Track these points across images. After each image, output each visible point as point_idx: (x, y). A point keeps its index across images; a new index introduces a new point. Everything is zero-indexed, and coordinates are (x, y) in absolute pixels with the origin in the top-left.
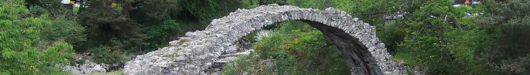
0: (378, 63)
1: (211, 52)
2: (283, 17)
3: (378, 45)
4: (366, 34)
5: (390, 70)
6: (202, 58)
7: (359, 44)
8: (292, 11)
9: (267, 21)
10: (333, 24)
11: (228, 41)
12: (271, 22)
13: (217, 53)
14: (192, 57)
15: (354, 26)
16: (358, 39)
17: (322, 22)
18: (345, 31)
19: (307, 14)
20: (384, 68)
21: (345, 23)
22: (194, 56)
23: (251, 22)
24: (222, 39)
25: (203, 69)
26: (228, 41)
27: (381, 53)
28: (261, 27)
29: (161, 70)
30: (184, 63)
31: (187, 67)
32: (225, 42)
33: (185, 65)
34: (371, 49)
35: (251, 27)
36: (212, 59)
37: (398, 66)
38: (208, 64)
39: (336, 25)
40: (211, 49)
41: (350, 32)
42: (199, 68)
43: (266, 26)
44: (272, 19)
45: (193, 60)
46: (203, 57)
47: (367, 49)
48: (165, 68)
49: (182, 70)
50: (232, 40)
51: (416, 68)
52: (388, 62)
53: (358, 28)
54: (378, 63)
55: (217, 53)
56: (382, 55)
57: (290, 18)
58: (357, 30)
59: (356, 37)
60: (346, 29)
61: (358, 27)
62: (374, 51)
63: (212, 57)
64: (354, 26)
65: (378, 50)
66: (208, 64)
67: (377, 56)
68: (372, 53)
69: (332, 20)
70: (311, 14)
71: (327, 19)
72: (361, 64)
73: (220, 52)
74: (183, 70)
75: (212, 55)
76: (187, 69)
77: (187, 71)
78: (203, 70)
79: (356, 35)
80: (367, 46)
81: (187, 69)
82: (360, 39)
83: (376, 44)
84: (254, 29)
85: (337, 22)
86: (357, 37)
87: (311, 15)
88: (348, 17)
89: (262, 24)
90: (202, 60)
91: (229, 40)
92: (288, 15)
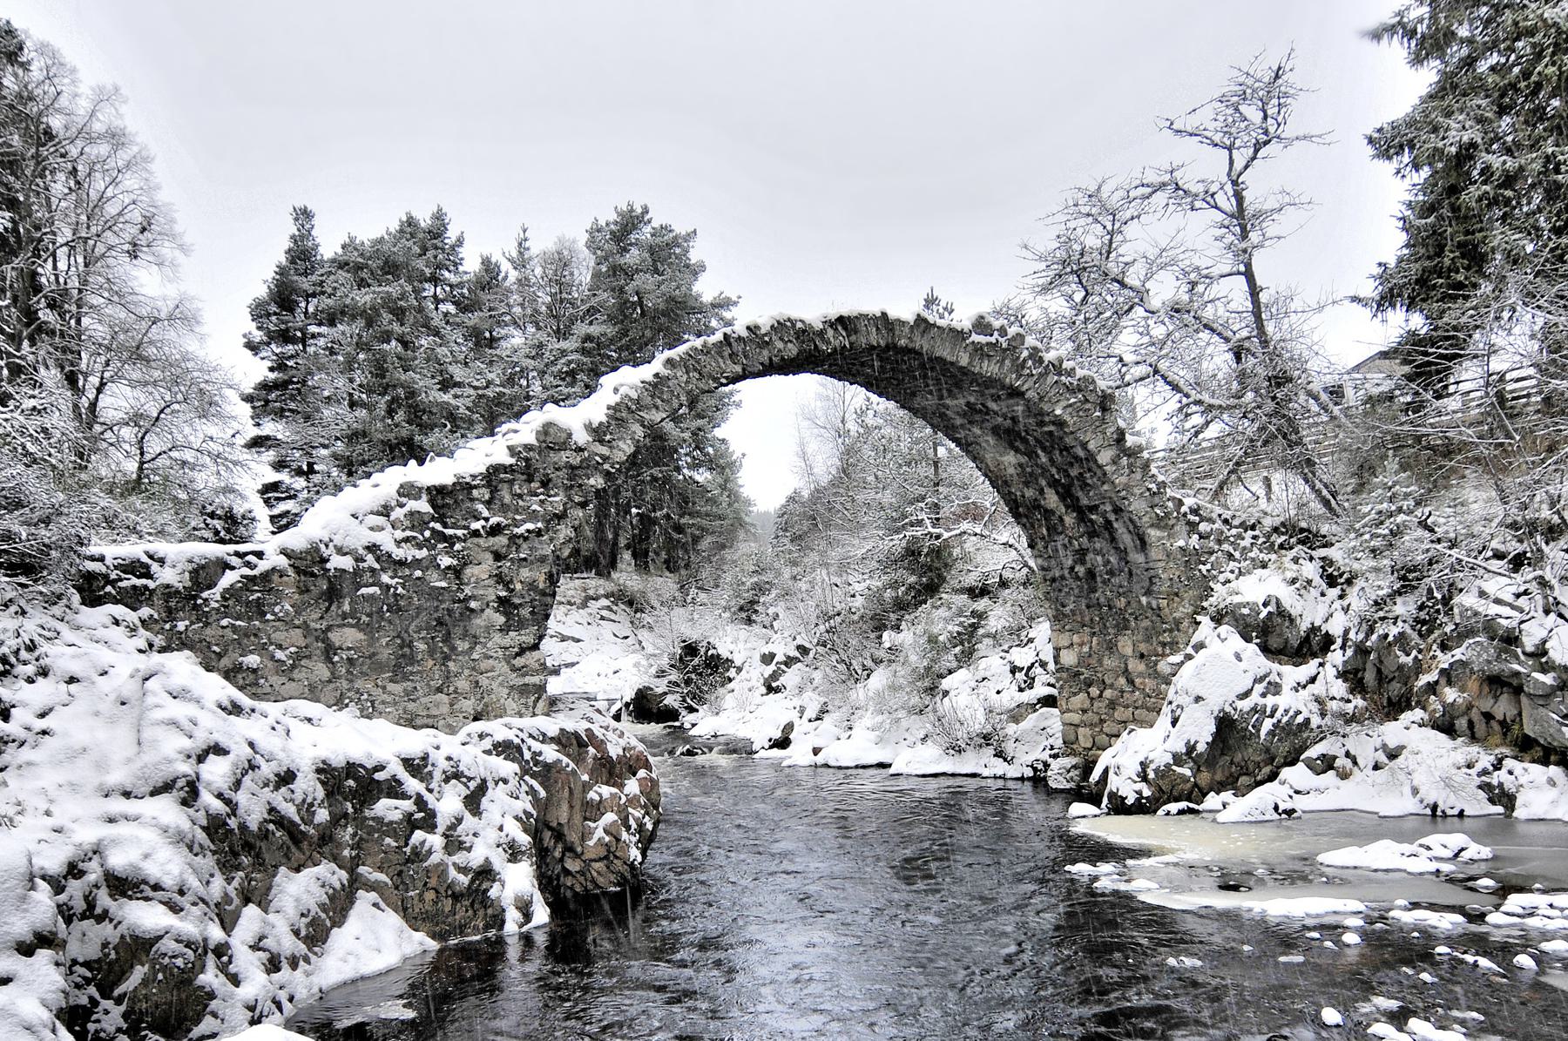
6: (571, 460)
9: (780, 345)
12: (792, 350)
13: (621, 444)
20: (1145, 519)
25: (577, 499)
26: (657, 408)
28: (762, 364)
31: (518, 491)
32: (648, 408)
35: (729, 362)
38: (592, 481)
63: (605, 459)
66: (592, 481)
68: (1107, 468)
72: (1069, 520)
73: (629, 442)
74: (507, 499)
75: (604, 450)
77: (521, 503)
81: (520, 496)
90: (573, 468)
91: (659, 402)
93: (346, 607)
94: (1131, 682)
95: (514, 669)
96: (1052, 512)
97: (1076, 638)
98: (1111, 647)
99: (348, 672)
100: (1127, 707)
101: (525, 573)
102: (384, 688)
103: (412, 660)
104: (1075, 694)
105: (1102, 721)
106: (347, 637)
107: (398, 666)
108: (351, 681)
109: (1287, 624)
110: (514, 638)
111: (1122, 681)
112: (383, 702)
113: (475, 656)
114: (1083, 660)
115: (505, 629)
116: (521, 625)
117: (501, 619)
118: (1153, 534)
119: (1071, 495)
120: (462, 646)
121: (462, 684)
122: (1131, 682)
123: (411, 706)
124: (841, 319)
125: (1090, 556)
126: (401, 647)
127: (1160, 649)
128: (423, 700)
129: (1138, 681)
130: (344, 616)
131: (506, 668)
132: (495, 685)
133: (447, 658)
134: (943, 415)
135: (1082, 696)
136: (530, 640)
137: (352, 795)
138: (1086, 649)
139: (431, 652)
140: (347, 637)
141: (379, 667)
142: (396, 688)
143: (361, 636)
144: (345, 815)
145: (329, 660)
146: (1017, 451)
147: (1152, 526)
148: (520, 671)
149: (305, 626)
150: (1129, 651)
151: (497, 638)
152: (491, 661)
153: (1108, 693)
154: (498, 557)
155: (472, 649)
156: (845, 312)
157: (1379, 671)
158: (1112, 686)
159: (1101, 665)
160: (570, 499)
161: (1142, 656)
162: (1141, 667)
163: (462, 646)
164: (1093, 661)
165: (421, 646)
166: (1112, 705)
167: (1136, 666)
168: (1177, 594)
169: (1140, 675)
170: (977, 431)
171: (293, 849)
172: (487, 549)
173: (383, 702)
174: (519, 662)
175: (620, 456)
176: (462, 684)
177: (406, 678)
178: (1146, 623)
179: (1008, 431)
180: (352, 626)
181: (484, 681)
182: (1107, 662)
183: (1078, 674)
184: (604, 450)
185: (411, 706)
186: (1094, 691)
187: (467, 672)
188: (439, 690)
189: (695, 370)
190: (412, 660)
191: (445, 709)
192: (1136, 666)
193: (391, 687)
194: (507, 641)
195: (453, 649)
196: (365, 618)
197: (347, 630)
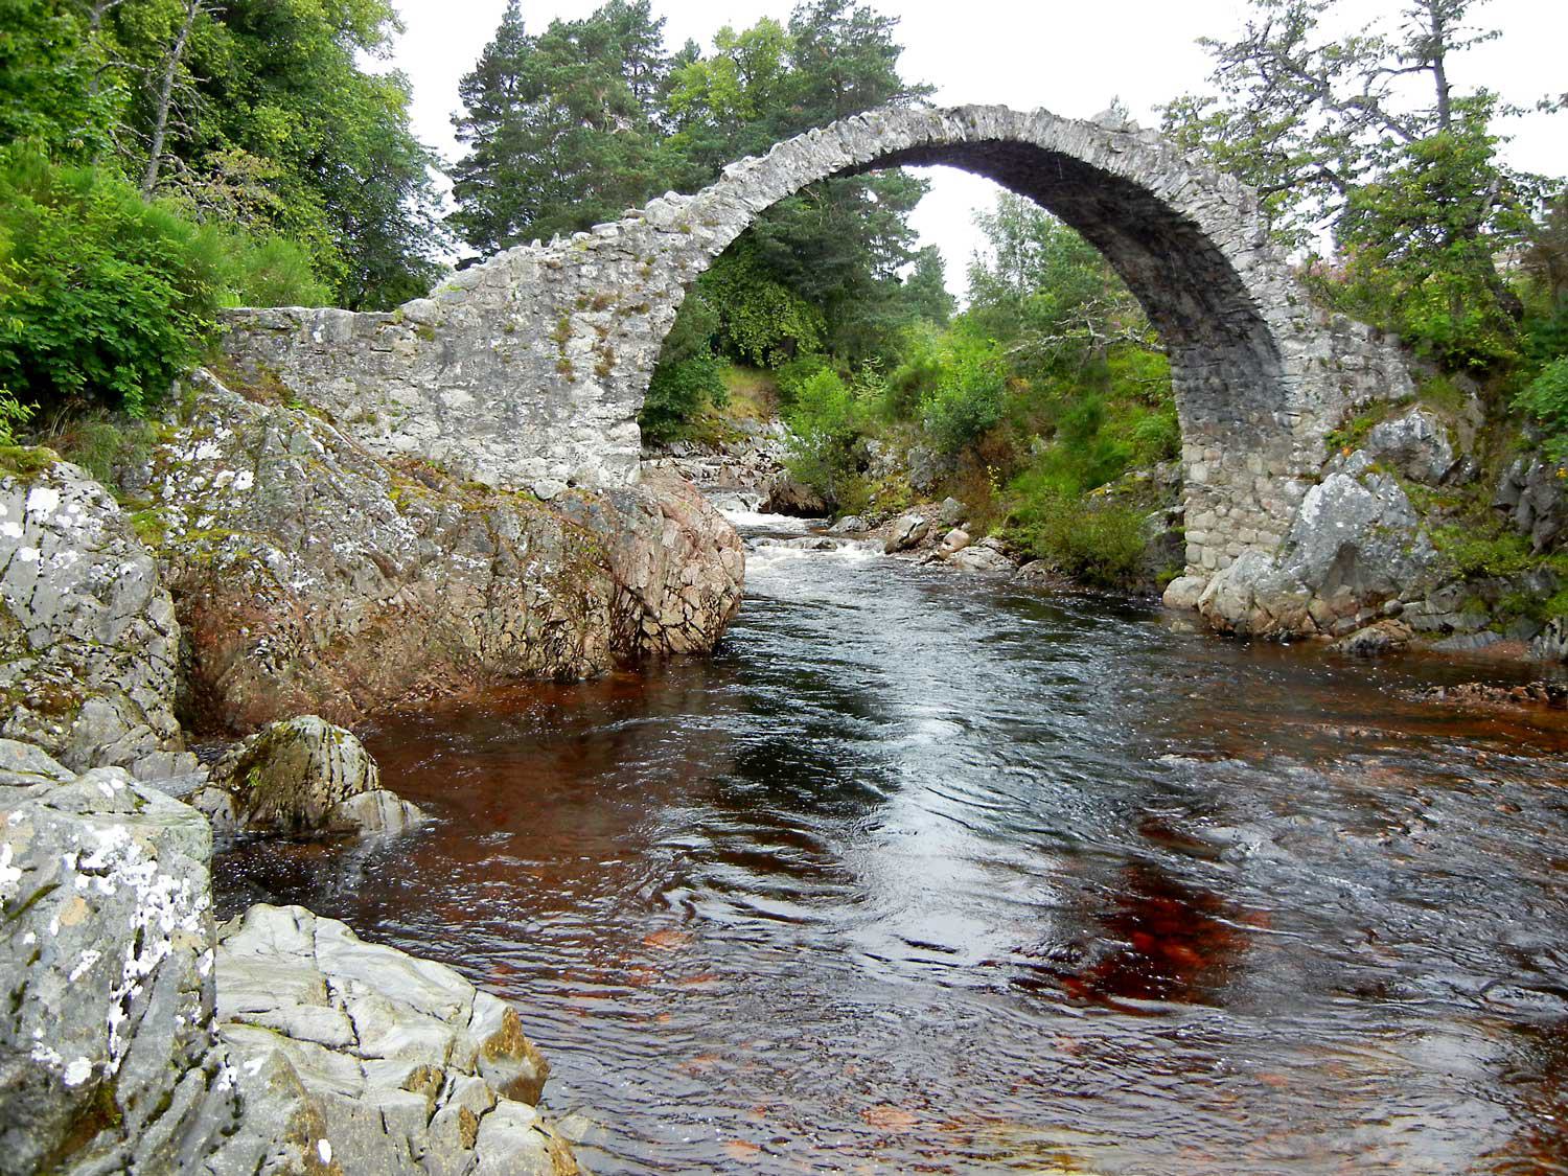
0: (1261, 311)
1: (706, 225)
2: (946, 123)
3: (1265, 250)
4: (1223, 208)
5: (1302, 336)
7: (1202, 243)
9: (892, 136)
10: (1116, 165)
11: (763, 194)
14: (641, 236)
15: (1184, 178)
16: (1195, 225)
17: (1076, 155)
18: (1152, 192)
19: (1028, 123)
20: (1282, 330)
21: (1154, 165)
22: (648, 233)
23: (841, 134)
25: (680, 280)
26: (763, 194)
27: (1271, 280)
30: (614, 256)
34: (1239, 263)
36: (711, 250)
37: (1327, 327)
38: (696, 264)
39: (1123, 167)
41: (1172, 199)
42: (666, 276)
43: (888, 151)
44: (911, 130)
45: (645, 246)
46: (681, 241)
47: (1224, 262)
49: (608, 276)
50: (776, 188)
51: (1388, 339)
52: (1297, 310)
53: (1196, 187)
54: (1261, 311)
55: (727, 229)
56: (1278, 283)
57: (971, 130)
59: (1191, 216)
60: (1160, 188)
61: (1198, 183)
62: (1251, 269)
63: (706, 243)
64: (1184, 178)
65: (1262, 268)
66: (696, 264)
67: (1260, 287)
69: (1112, 151)
70: (1043, 123)
71: (1096, 143)
74: (614, 277)
75: (708, 234)
78: (682, 285)
79: (1190, 210)
80: (1225, 250)
81: (626, 275)
82: (1204, 223)
83: (1258, 246)
84: (849, 159)
86: (1199, 218)
87: (1039, 125)
88: (1165, 146)
89: (878, 144)
90: (677, 249)
91: (766, 189)
92: (962, 120)
93: (458, 370)
94: (1257, 502)
95: (610, 439)
96: (1188, 318)
97: (1207, 453)
98: (1241, 464)
99: (456, 430)
100: (1251, 527)
102: (487, 447)
104: (1203, 511)
105: (1227, 541)
106: (457, 398)
107: (502, 427)
108: (458, 439)
109: (1432, 451)
110: (610, 410)
111: (1249, 500)
112: (485, 461)
113: (573, 424)
114: (1214, 478)
115: (602, 401)
116: (617, 400)
117: (600, 391)
119: (1205, 301)
120: (562, 413)
121: (560, 450)
122: (1257, 502)
123: (511, 466)
124: (957, 111)
125: (1225, 366)
126: (506, 410)
127: (1288, 469)
128: (524, 462)
129: (1264, 501)
130: (456, 378)
131: (602, 437)
132: (589, 454)
133: (547, 424)
134: (1077, 212)
135: (1209, 513)
136: (627, 414)
138: (1216, 464)
139: (533, 417)
140: (457, 398)
141: (483, 428)
142: (500, 449)
143: (470, 398)
145: (439, 418)
146: (1153, 253)
147: (1290, 337)
150: (1258, 468)
151: (595, 409)
152: (588, 430)
153: (1235, 512)
154: (601, 331)
155: (570, 417)
156: (962, 104)
157: (1533, 509)
158: (1238, 504)
159: (1230, 482)
161: (1270, 475)
162: (1269, 486)
163: (562, 413)
164: (1222, 477)
165: (524, 411)
166: (1238, 525)
167: (1265, 485)
168: (1311, 412)
169: (1267, 495)
170: (1112, 230)
171: (384, 581)
172: (591, 324)
173: (485, 461)
174: (614, 432)
177: (507, 440)
178: (1277, 440)
179: (1144, 231)
180: (459, 387)
181: (580, 448)
182: (1237, 479)
183: (1207, 491)
184: (708, 234)
185: (511, 466)
186: (1221, 509)
187: (565, 439)
188: (538, 453)
189: (804, 159)
190: (515, 424)
191: (543, 472)
192: (1265, 485)
193: (493, 447)
194: (603, 413)
195: (553, 415)
197: (457, 391)
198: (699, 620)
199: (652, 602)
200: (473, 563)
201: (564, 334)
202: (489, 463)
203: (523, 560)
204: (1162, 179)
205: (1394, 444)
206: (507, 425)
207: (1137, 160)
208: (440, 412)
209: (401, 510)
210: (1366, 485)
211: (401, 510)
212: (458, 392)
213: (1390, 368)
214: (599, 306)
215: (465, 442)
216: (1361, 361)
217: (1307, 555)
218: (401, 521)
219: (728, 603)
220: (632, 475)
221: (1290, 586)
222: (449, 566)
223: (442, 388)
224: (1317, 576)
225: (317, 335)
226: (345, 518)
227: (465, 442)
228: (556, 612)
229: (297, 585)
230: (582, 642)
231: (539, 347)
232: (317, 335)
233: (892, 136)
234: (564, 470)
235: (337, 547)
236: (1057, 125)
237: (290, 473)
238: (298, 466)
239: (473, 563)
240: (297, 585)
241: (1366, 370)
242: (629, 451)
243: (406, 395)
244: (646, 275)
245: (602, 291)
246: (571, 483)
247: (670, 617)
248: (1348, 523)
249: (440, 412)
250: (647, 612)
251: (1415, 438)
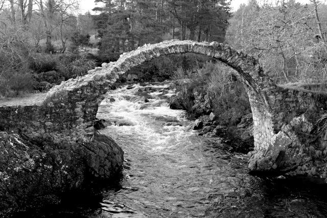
2: (169, 50)
8: (177, 45)
9: (155, 54)
24: (117, 69)
29: (67, 93)
33: (87, 89)
40: (109, 77)
48: (70, 92)
56: (266, 81)
58: (240, 60)
63: (109, 83)
64: (237, 57)
65: (261, 78)
67: (261, 82)
70: (196, 47)
74: (86, 93)
75: (109, 81)
76: (88, 92)
80: (250, 74)
81: (88, 92)
84: (144, 60)
85: (220, 54)
89: (151, 56)
90: (101, 85)
101: (89, 110)
103: (63, 129)
106: (49, 123)
116: (88, 121)
118: (271, 97)
120: (74, 126)
121: (74, 134)
122: (266, 135)
130: (49, 119)
133: (70, 128)
136: (90, 124)
137: (41, 162)
139: (67, 127)
140: (49, 123)
141: (55, 130)
142: (59, 135)
143: (52, 124)
144: (40, 166)
148: (88, 131)
149: (40, 121)
151: (82, 124)
155: (76, 126)
160: (100, 92)
175: (112, 82)
176: (74, 134)
177: (61, 133)
181: (78, 133)
184: (109, 81)
185: (62, 139)
188: (68, 135)
190: (63, 129)
193: (58, 134)
194: (84, 125)
195: (72, 126)
196: (53, 120)
198: (108, 173)
199: (96, 170)
200: (48, 167)
201: (74, 107)
202: (57, 138)
203: (61, 165)
204: (230, 58)
205: (297, 123)
206: (60, 130)
207: (223, 54)
208: (45, 127)
209: (31, 157)
210: (287, 135)
211: (31, 157)
212: (50, 123)
213: (300, 101)
214: (83, 100)
215: (51, 134)
216: (291, 99)
217: (272, 154)
218: (31, 160)
219: (117, 168)
220: (92, 139)
221: (266, 162)
222: (43, 167)
223: (45, 122)
224: (274, 159)
225: (16, 112)
226: (17, 162)
227: (51, 134)
228: (69, 177)
229: (5, 179)
230: (75, 183)
231: (68, 111)
232: (16, 112)
233: (155, 54)
234: (75, 139)
235: (15, 169)
236: (200, 48)
237: (5, 152)
238: (7, 151)
239: (48, 167)
240: (5, 179)
241: (293, 102)
242: (91, 133)
243: (37, 124)
244: (94, 92)
245: (83, 96)
246: (77, 141)
247: (102, 173)
248: (282, 145)
249: (45, 127)
250: (95, 172)
251: (303, 122)
